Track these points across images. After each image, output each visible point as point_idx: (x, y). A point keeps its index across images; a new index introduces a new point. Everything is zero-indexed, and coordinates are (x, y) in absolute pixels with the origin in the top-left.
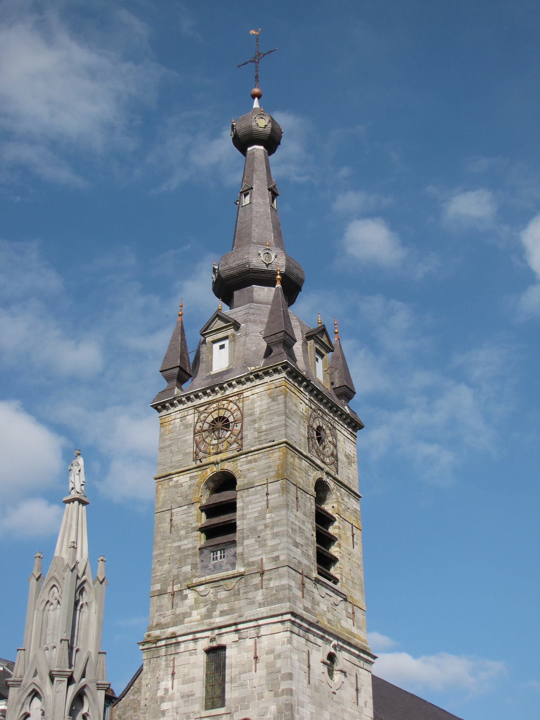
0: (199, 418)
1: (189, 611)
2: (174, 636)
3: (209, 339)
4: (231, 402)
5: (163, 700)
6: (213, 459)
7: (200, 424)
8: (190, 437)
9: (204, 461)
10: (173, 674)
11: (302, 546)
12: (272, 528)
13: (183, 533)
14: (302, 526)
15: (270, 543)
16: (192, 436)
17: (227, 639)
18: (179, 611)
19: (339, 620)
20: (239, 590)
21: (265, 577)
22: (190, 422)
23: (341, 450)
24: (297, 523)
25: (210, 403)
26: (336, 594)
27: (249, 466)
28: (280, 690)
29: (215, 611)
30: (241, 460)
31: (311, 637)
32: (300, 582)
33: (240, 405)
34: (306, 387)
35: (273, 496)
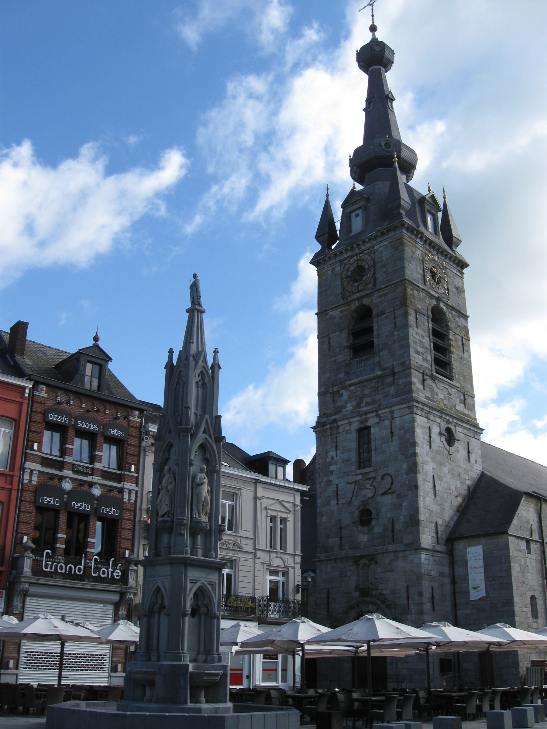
1: (344, 404)
2: (335, 421)
4: (366, 254)
5: (330, 464)
6: (355, 296)
7: (345, 273)
8: (338, 283)
9: (349, 299)
10: (336, 447)
11: (422, 354)
13: (337, 351)
14: (421, 339)
15: (399, 353)
16: (340, 282)
17: (372, 421)
18: (338, 404)
19: (454, 406)
20: (378, 387)
21: (396, 377)
22: (338, 272)
23: (451, 283)
24: (418, 337)
25: (352, 256)
26: (451, 387)
27: (381, 299)
28: (409, 454)
29: (362, 403)
30: (375, 295)
31: (431, 417)
32: (421, 379)
33: (372, 255)
34: (421, 238)
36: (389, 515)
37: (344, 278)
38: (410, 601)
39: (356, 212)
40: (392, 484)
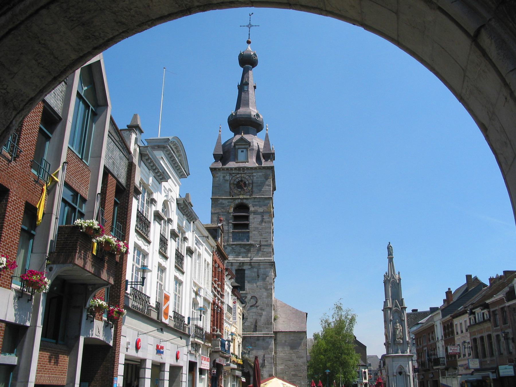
0: (232, 178)
3: (237, 147)
8: (228, 185)
16: (229, 185)
33: (252, 178)
36: (254, 317)
37: (232, 184)
38: (266, 362)
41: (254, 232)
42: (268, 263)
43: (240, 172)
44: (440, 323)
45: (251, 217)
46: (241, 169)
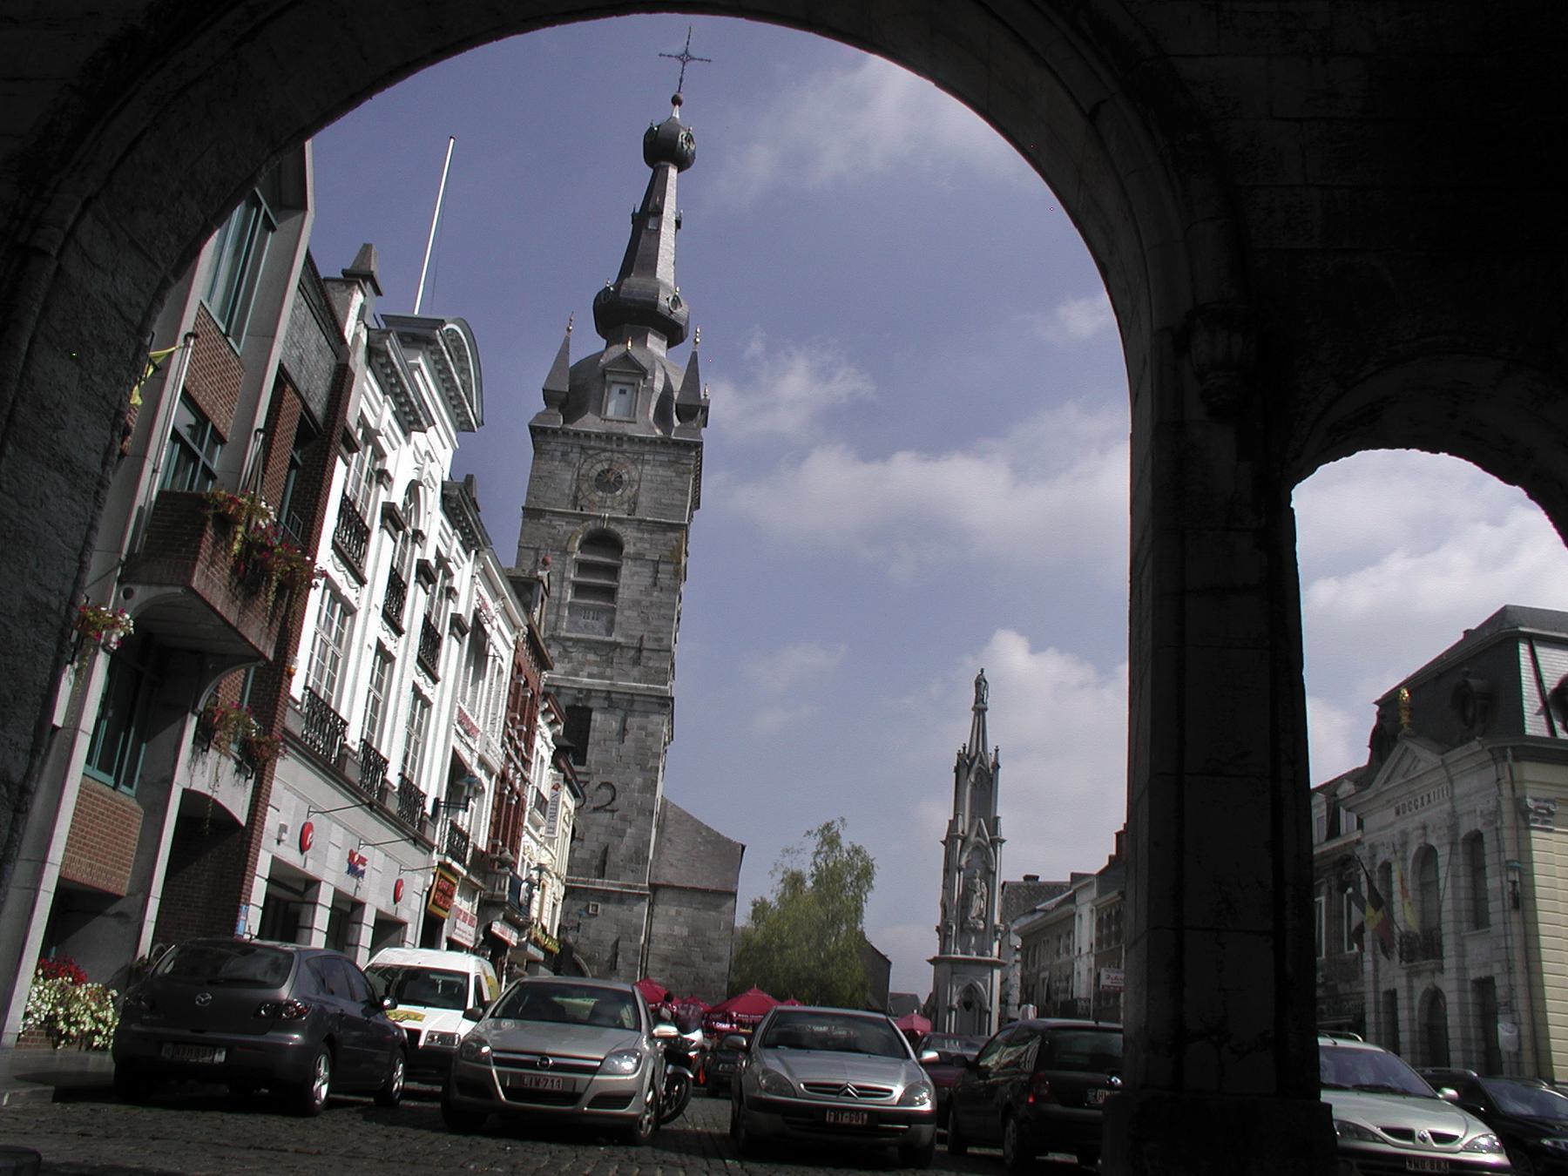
12: (660, 608)
15: (655, 623)
35: (663, 576)
36: (602, 839)
38: (619, 959)
39: (624, 387)
40: (613, 799)
41: (627, 613)
42: (654, 700)
43: (609, 447)
44: (1092, 911)
45: (624, 571)
46: (615, 438)
